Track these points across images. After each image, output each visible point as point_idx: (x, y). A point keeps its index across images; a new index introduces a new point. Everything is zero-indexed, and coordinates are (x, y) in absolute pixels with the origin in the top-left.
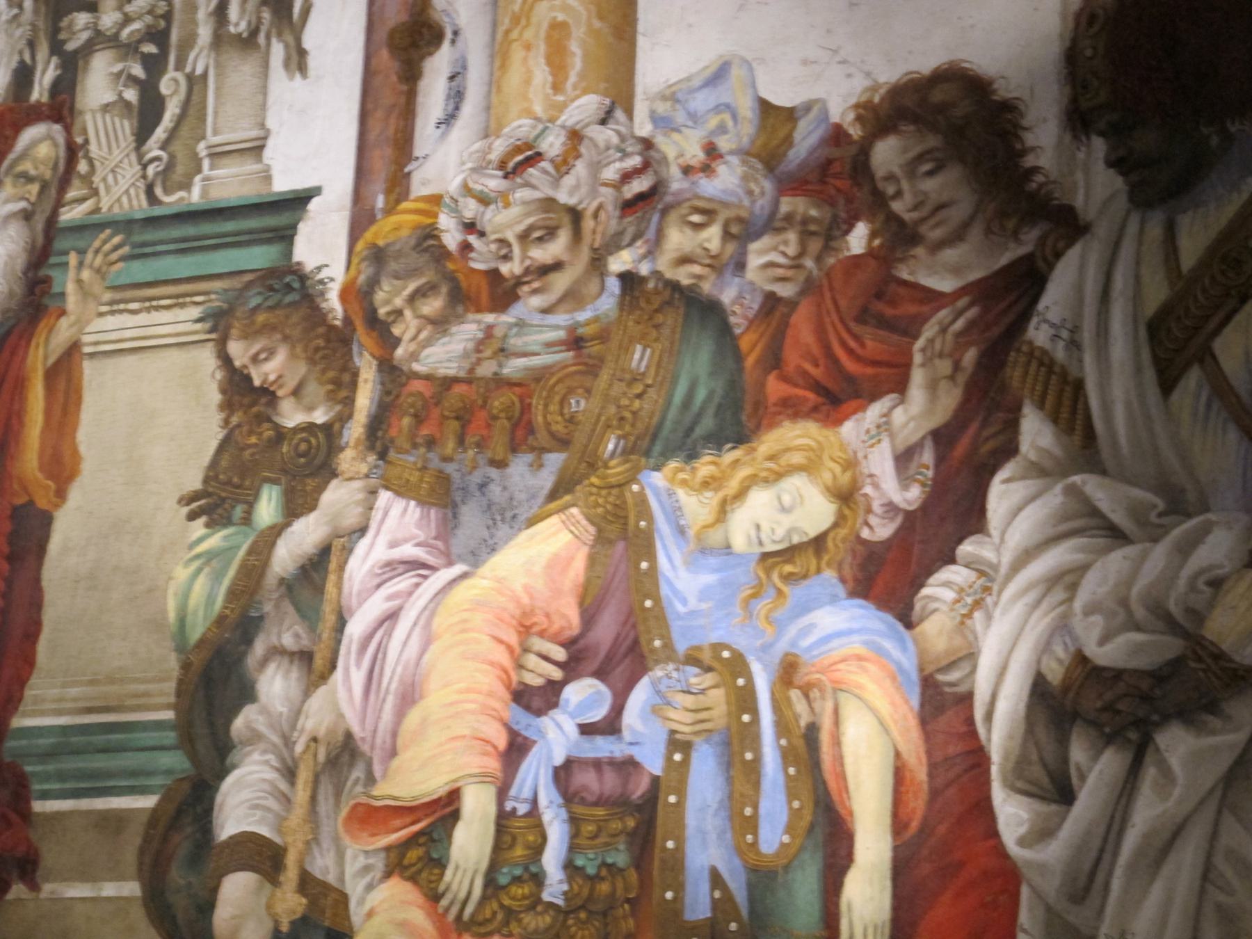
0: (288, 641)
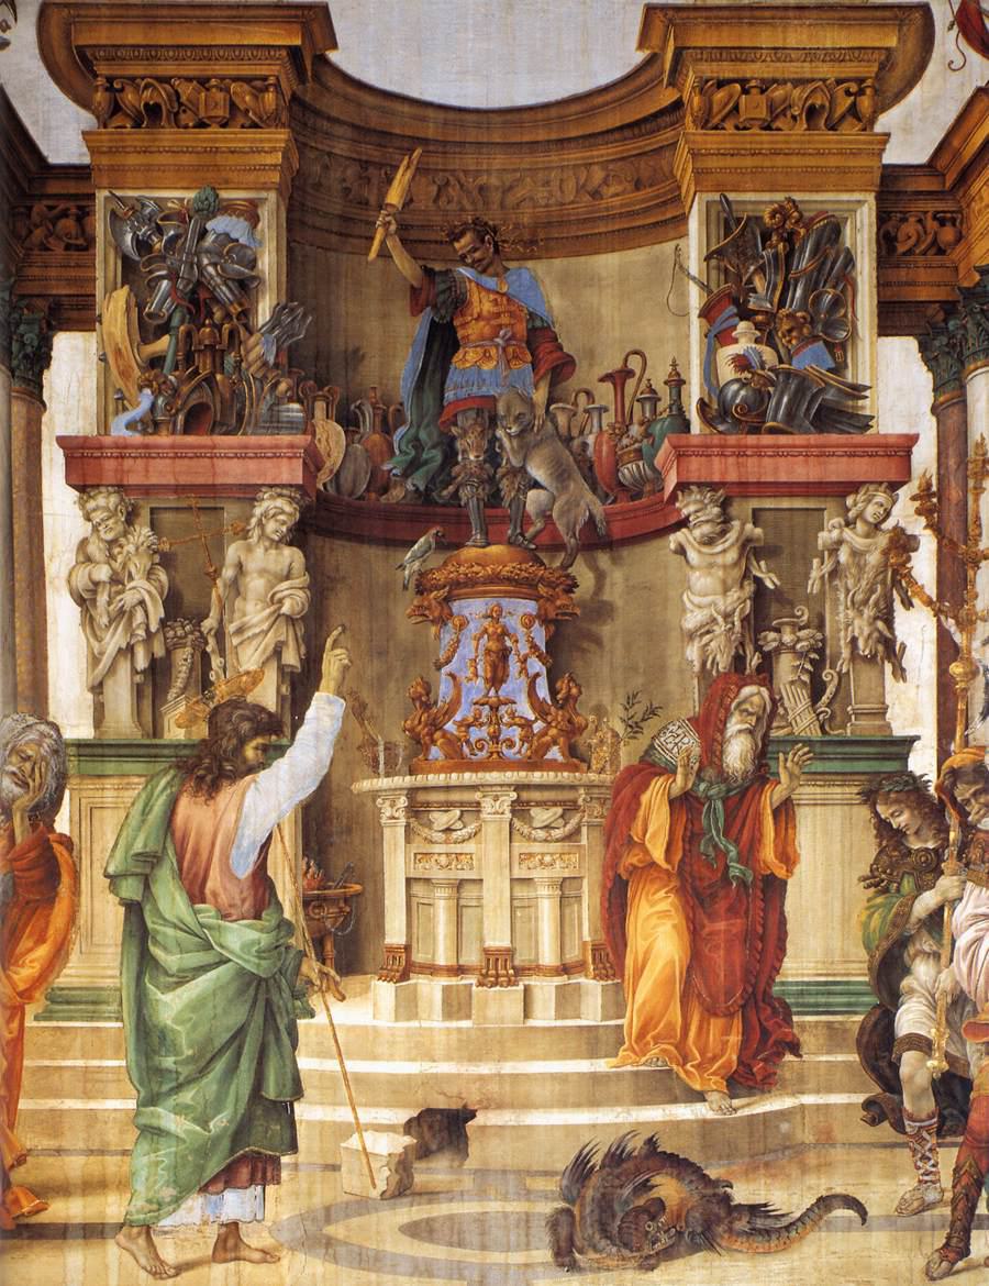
0: (926, 948)
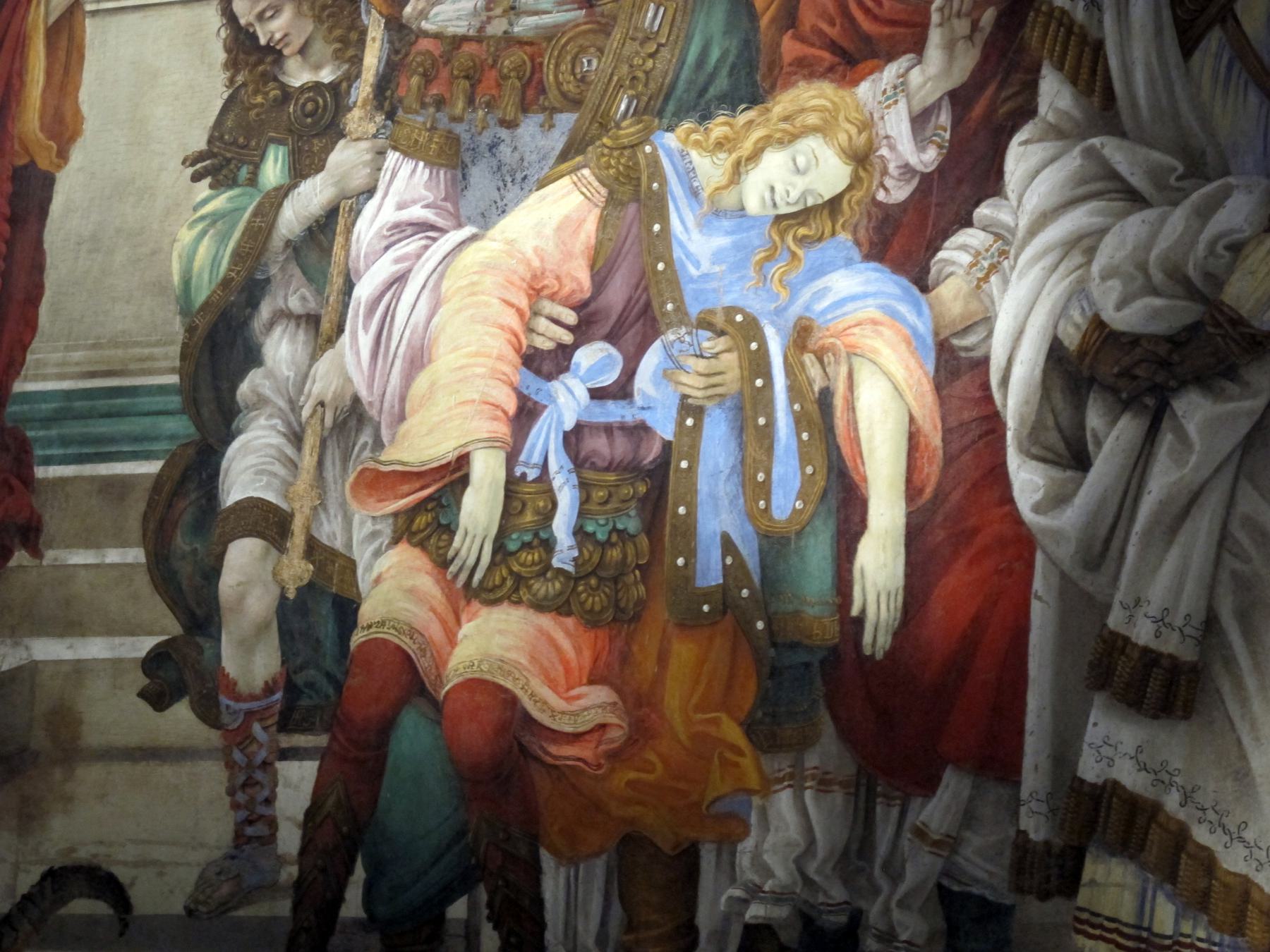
0: (294, 304)
